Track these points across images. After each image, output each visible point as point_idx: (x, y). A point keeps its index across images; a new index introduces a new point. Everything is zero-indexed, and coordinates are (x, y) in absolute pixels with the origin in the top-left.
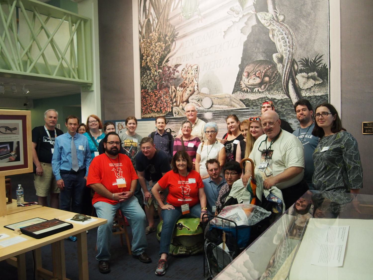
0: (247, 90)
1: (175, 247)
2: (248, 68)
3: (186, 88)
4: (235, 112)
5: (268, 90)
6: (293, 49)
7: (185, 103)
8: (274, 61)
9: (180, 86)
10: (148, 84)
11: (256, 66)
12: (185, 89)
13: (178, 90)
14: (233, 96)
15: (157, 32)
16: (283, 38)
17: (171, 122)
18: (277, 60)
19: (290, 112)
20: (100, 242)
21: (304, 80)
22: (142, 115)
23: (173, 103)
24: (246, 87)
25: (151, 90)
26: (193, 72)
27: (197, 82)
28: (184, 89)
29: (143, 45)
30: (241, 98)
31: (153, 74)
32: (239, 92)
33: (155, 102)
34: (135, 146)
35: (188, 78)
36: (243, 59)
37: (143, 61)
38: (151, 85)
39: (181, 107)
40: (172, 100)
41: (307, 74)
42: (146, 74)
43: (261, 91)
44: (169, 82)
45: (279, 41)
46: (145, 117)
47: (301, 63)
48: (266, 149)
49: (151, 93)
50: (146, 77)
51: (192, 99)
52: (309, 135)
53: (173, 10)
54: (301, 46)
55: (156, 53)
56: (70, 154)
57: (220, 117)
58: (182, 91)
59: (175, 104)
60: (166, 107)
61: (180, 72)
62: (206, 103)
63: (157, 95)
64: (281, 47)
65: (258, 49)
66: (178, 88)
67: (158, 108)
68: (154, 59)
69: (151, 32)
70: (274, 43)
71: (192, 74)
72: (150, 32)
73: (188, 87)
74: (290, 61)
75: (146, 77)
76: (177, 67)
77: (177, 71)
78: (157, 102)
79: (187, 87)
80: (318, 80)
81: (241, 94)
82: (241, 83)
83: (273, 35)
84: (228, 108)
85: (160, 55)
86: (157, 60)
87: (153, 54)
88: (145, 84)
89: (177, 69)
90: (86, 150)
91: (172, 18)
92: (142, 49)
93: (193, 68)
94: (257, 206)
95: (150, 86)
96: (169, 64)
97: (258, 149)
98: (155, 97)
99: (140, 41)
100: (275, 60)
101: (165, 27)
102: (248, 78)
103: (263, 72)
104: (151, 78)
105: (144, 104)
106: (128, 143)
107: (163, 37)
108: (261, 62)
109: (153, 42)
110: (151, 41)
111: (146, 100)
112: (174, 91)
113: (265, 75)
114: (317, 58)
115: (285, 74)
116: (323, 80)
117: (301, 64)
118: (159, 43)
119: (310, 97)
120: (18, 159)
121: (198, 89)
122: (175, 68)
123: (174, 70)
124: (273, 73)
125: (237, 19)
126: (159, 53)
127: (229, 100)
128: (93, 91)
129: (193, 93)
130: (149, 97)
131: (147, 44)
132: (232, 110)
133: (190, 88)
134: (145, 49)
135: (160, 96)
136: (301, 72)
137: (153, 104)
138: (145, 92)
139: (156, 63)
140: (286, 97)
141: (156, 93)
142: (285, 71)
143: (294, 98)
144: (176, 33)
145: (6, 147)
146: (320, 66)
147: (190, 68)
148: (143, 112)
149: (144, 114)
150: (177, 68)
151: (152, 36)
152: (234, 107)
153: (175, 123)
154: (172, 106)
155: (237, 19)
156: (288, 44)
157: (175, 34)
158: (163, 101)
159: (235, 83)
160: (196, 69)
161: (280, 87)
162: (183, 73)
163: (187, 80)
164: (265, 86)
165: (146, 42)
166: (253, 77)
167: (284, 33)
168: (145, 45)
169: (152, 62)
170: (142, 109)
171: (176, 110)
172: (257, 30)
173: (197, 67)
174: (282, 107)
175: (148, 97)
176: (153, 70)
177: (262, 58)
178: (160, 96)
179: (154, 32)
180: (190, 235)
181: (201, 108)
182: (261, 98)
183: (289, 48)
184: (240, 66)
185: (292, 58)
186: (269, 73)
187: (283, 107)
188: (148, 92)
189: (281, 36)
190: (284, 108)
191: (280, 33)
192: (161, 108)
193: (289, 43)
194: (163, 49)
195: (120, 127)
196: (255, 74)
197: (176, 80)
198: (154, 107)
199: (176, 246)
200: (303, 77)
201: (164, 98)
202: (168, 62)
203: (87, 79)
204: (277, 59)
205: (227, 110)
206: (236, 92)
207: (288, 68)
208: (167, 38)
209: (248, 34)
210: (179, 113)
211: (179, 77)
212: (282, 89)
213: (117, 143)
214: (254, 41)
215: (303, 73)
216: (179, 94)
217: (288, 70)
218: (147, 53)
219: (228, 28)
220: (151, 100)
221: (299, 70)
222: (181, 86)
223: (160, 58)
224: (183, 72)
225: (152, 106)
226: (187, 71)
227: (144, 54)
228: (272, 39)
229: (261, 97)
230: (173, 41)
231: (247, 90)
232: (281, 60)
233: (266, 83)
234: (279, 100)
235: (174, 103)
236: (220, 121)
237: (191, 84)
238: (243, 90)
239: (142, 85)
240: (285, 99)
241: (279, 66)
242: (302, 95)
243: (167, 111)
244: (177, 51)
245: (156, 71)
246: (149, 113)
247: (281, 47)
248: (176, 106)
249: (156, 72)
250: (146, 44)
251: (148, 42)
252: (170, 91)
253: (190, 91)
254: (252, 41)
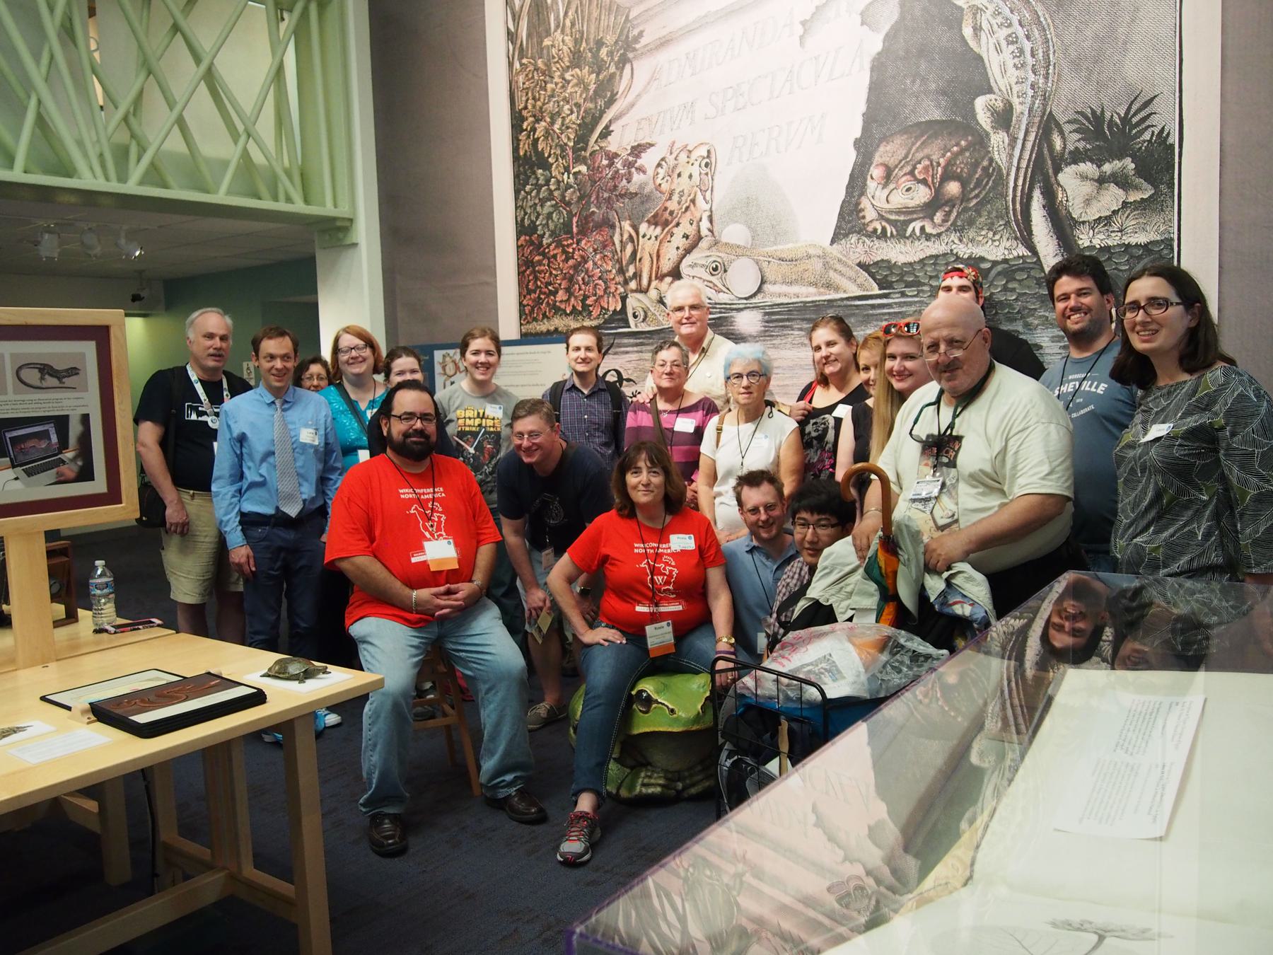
0: (884, 229)
1: (628, 770)
2: (888, 152)
3: (670, 227)
4: (839, 306)
5: (955, 228)
6: (1046, 77)
7: (668, 279)
8: (978, 123)
9: (648, 221)
10: (541, 217)
11: (913, 144)
12: (668, 232)
13: (644, 236)
14: (835, 250)
15: (568, 31)
16: (1012, 40)
17: (620, 346)
18: (989, 121)
19: (1034, 304)
20: (371, 753)
21: (1088, 188)
22: (521, 324)
23: (626, 282)
24: (881, 217)
25: (550, 236)
26: (695, 170)
27: (707, 207)
28: (663, 230)
29: (521, 79)
30: (864, 259)
31: (558, 182)
32: (854, 238)
33: (563, 279)
34: (492, 429)
35: (677, 191)
36: (869, 119)
37: (523, 136)
38: (552, 219)
39: (653, 293)
40: (622, 271)
41: (1099, 167)
42: (532, 181)
43: (934, 232)
44: (612, 208)
45: (998, 50)
46: (533, 331)
47: (1075, 126)
48: (936, 433)
49: (552, 247)
50: (534, 194)
51: (693, 266)
52: (1096, 383)
54: (1076, 65)
55: (567, 107)
56: (271, 460)
57: (787, 327)
58: (656, 237)
59: (633, 285)
60: (602, 296)
61: (650, 172)
62: (742, 280)
63: (573, 253)
64: (1004, 72)
65: (924, 80)
66: (643, 228)
67: (576, 298)
68: (560, 129)
69: (548, 34)
70: (980, 58)
71: (690, 176)
72: (544, 35)
73: (678, 225)
74: (1037, 120)
75: (534, 194)
76: (640, 152)
77: (641, 170)
78: (571, 280)
79: (674, 223)
80: (1137, 188)
81: (864, 242)
82: (862, 206)
83: (977, 29)
84: (815, 295)
85: (578, 112)
86: (570, 130)
87: (557, 110)
88: (530, 216)
89: (639, 162)
90: (327, 444)
92: (518, 94)
93: (694, 155)
94: (898, 631)
95: (547, 224)
96: (613, 144)
97: (911, 433)
98: (566, 260)
99: (511, 65)
100: (984, 119)
101: (595, 14)
102: (885, 186)
103: (939, 164)
104: (551, 196)
105: (527, 285)
106: (470, 418)
107: (590, 50)
108: (931, 129)
109: (554, 69)
110: (548, 65)
111: (534, 272)
112: (631, 236)
113: (947, 177)
114: (1134, 108)
115: (1018, 169)
116: (1156, 187)
117: (1075, 131)
118: (577, 70)
119: (1106, 249)
120: (86, 474)
121: (711, 231)
122: (631, 159)
123: (629, 165)
124: (976, 165)
126: (578, 106)
127: (817, 265)
128: (355, 245)
129: (694, 243)
130: (545, 262)
131: (536, 77)
132: (829, 301)
134: (527, 94)
135: (582, 257)
136: (1075, 162)
137: (560, 285)
138: (531, 243)
139: (566, 141)
140: (1022, 251)
141: (568, 246)
142: (1020, 159)
143: (1052, 255)
144: (636, 32)
145: (45, 435)
146: (1147, 136)
147: (683, 157)
148: (525, 314)
149: (528, 322)
150: (638, 156)
151: (553, 46)
152: (837, 289)
153: (635, 349)
154: (622, 290)
156: (1030, 61)
157: (630, 35)
158: (593, 276)
159: (842, 207)
160: (704, 158)
161: (999, 217)
162: (660, 176)
163: (676, 198)
164: (948, 214)
165: (531, 68)
166: (905, 182)
167: (1015, 19)
168: (528, 80)
169: (552, 140)
170: (520, 303)
171: (636, 304)
172: (918, 13)
173: (709, 152)
174: (1005, 289)
175: (540, 263)
176: (557, 167)
177: (936, 115)
178: (582, 257)
179: (559, 31)
180: (675, 730)
181: (723, 298)
182: (931, 257)
183: (1034, 73)
184: (857, 144)
185: (1045, 110)
187: (1010, 286)
188: (541, 244)
189: (1006, 32)
190: (1013, 290)
191: (1000, 20)
192: (586, 297)
193: (1033, 56)
194: (591, 92)
195: (450, 369)
196: (912, 173)
197: (637, 200)
198: (561, 295)
199: (632, 768)
200: (1084, 177)
201: (595, 264)
202: (609, 138)
203: (335, 206)
204: (989, 114)
205: (812, 302)
206: (846, 235)
207: (1029, 145)
208: (603, 52)
209: (886, 28)
210: (649, 314)
211: (647, 190)
212: (1007, 224)
213: (424, 417)
214: (907, 52)
215: (1082, 165)
216: (647, 247)
217: (1031, 155)
218: (534, 106)
219: (817, 8)
220: (551, 273)
221: (1070, 152)
222: (654, 221)
223: (579, 125)
224: (659, 170)
225: (555, 293)
226: (675, 167)
227: (525, 113)
228: (972, 44)
229: (934, 252)
230: (624, 61)
231: (884, 229)
232: (1004, 118)
233: (951, 202)
234: (995, 263)
235: (631, 279)
236: (790, 339)
237: (688, 213)
238: (870, 229)
239: (519, 219)
240: (1019, 257)
241: (998, 140)
242: (1080, 242)
243: (608, 310)
244: (639, 96)
245: (567, 169)
246: (545, 316)
247: (1004, 72)
248: (636, 291)
249: (566, 176)
250: (533, 77)
251: (537, 69)
252: (617, 239)
253: (684, 237)
254: (901, 53)
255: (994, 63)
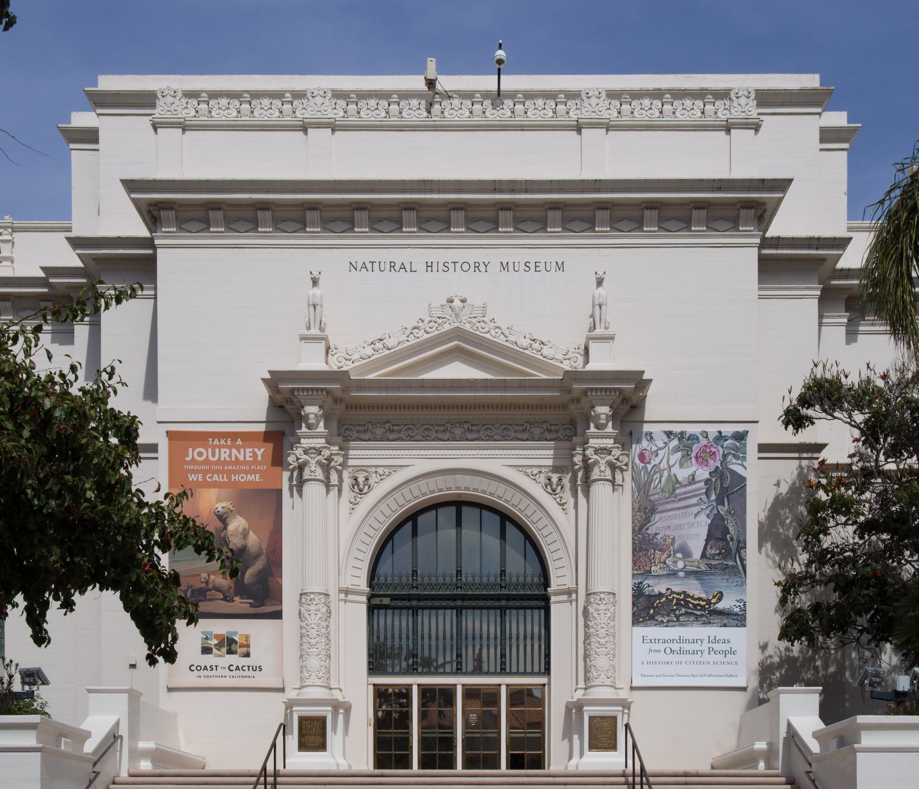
2: (712, 542)
5: (724, 559)
16: (733, 526)
23: (651, 563)
26: (670, 541)
36: (708, 535)
39: (658, 566)
53: (653, 489)
66: (656, 552)
77: (657, 539)
91: (652, 495)
96: (649, 532)
100: (728, 539)
113: (722, 549)
123: (653, 537)
125: (704, 507)
133: (667, 552)
140: (735, 564)
155: (704, 507)
166: (714, 549)
181: (676, 568)
184: (705, 540)
186: (725, 547)
208: (647, 510)
216: (657, 556)
222: (659, 550)
230: (652, 514)
232: (732, 539)
233: (723, 553)
241: (731, 543)
245: (636, 536)
255: (730, 529)
